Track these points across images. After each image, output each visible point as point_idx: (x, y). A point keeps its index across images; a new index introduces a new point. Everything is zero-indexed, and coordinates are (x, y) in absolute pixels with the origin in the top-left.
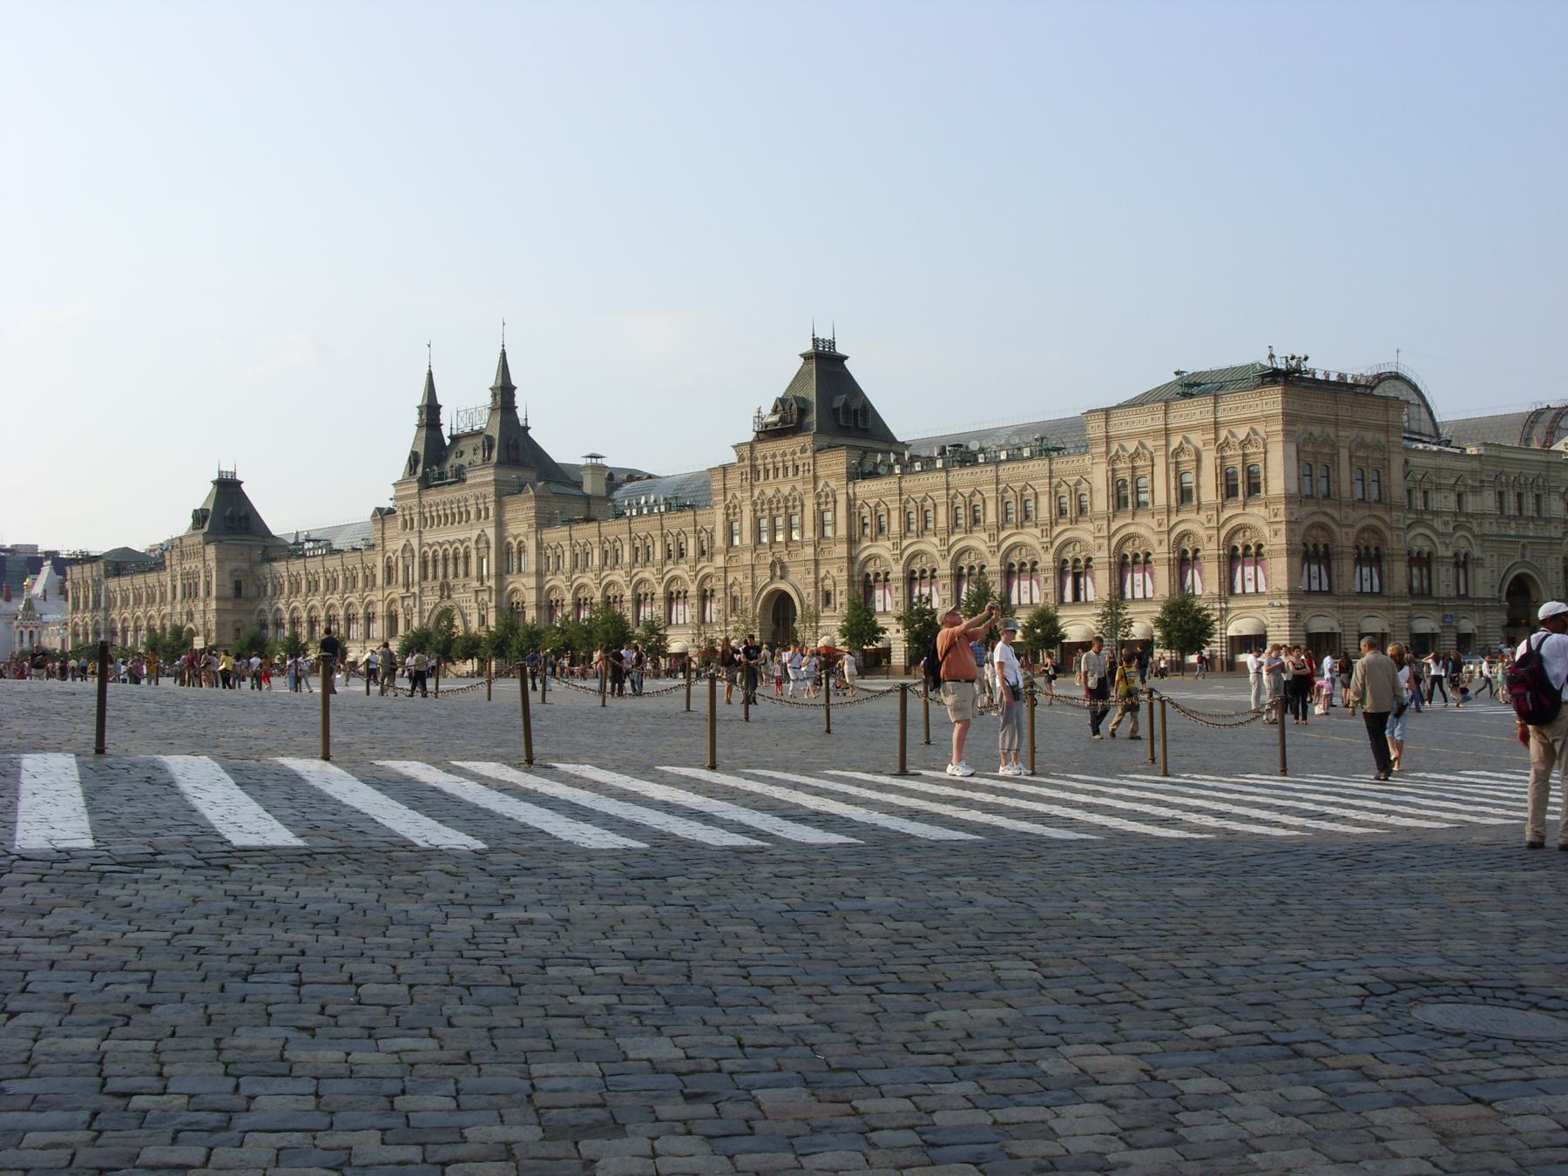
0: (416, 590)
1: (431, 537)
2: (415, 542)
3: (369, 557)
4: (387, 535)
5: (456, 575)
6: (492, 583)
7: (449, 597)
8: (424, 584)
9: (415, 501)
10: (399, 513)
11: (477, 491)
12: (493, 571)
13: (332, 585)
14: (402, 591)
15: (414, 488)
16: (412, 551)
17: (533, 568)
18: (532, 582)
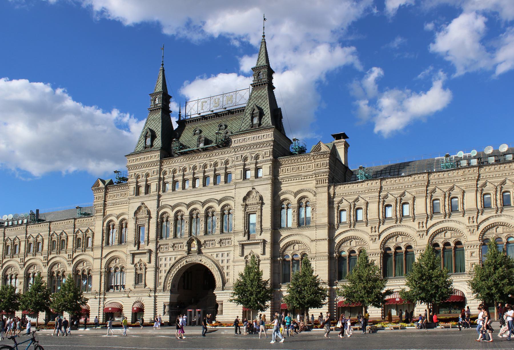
0: (152, 246)
1: (169, 199)
2: (152, 205)
3: (83, 224)
4: (109, 201)
5: (206, 233)
6: (267, 236)
7: (199, 252)
8: (161, 242)
9: (157, 168)
10: (132, 180)
11: (246, 153)
12: (267, 223)
13: (33, 247)
14: (133, 248)
15: (156, 156)
16: (149, 213)
17: (325, 220)
18: (324, 233)
